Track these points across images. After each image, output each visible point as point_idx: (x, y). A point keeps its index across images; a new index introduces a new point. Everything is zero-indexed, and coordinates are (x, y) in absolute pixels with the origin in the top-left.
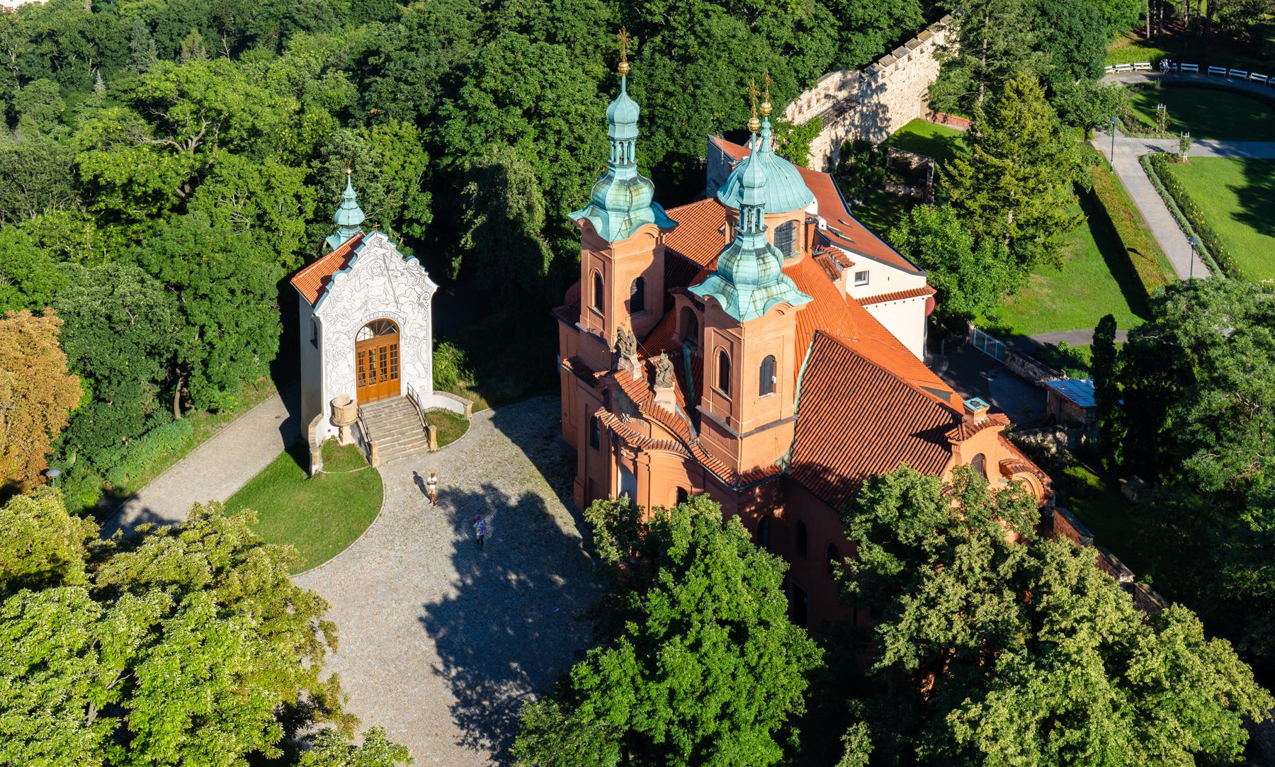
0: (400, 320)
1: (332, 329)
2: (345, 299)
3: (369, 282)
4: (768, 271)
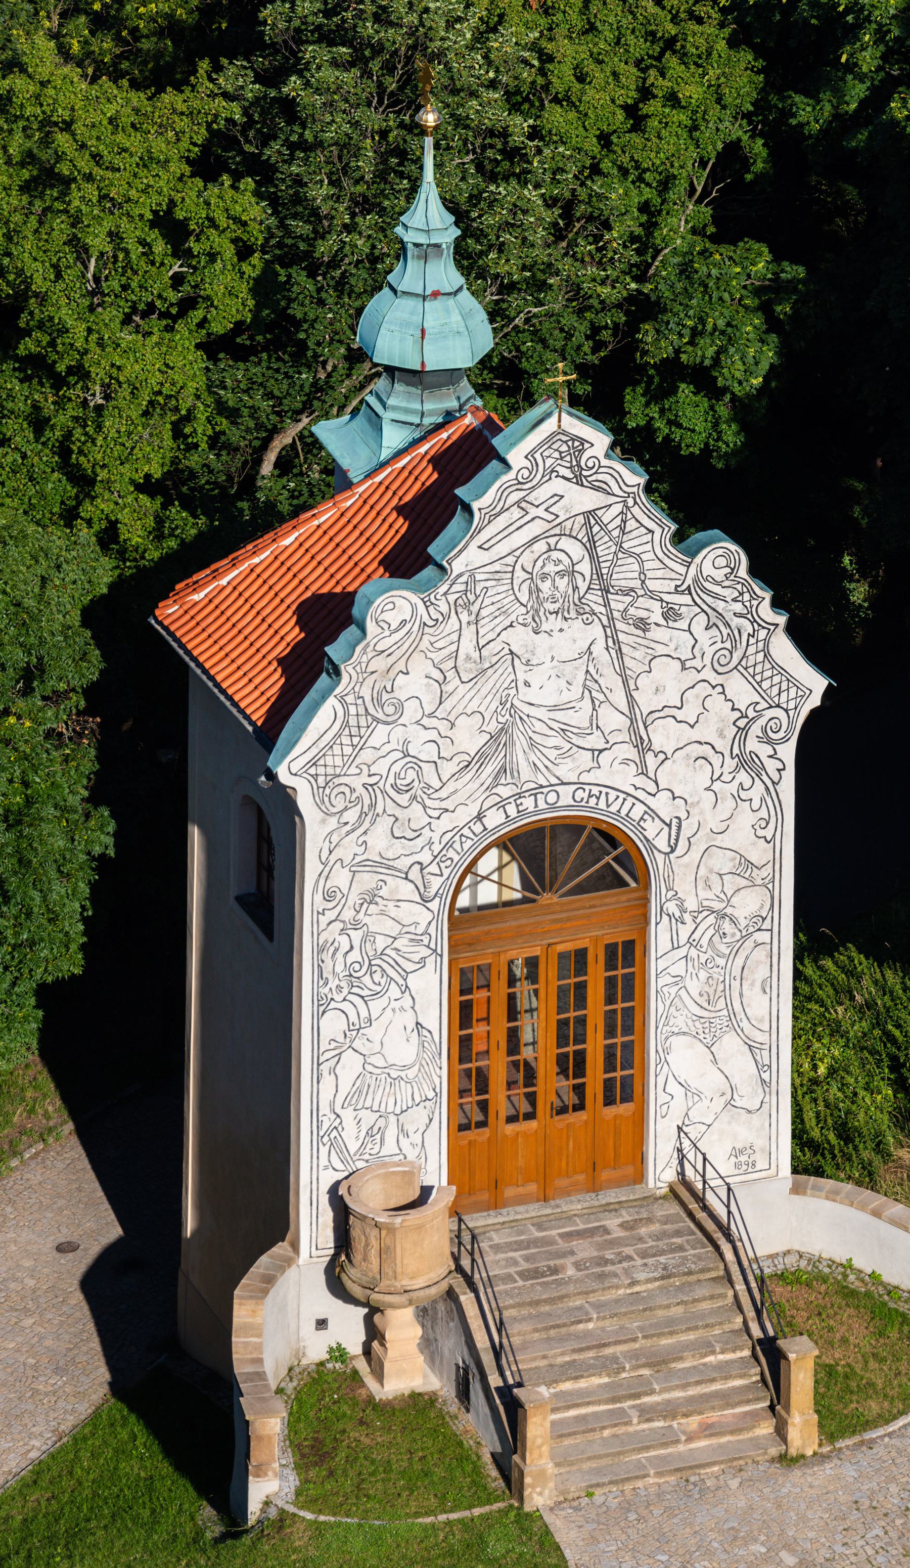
0: (651, 828)
1: (348, 850)
2: (411, 711)
3: (519, 638)
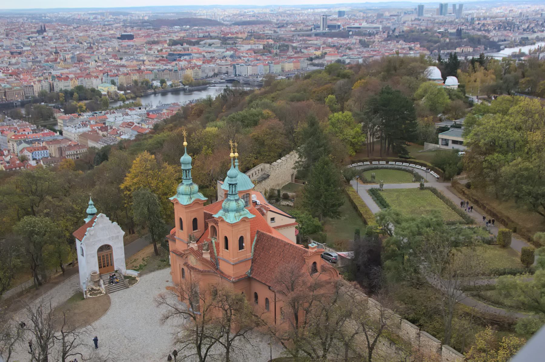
4: (240, 207)
